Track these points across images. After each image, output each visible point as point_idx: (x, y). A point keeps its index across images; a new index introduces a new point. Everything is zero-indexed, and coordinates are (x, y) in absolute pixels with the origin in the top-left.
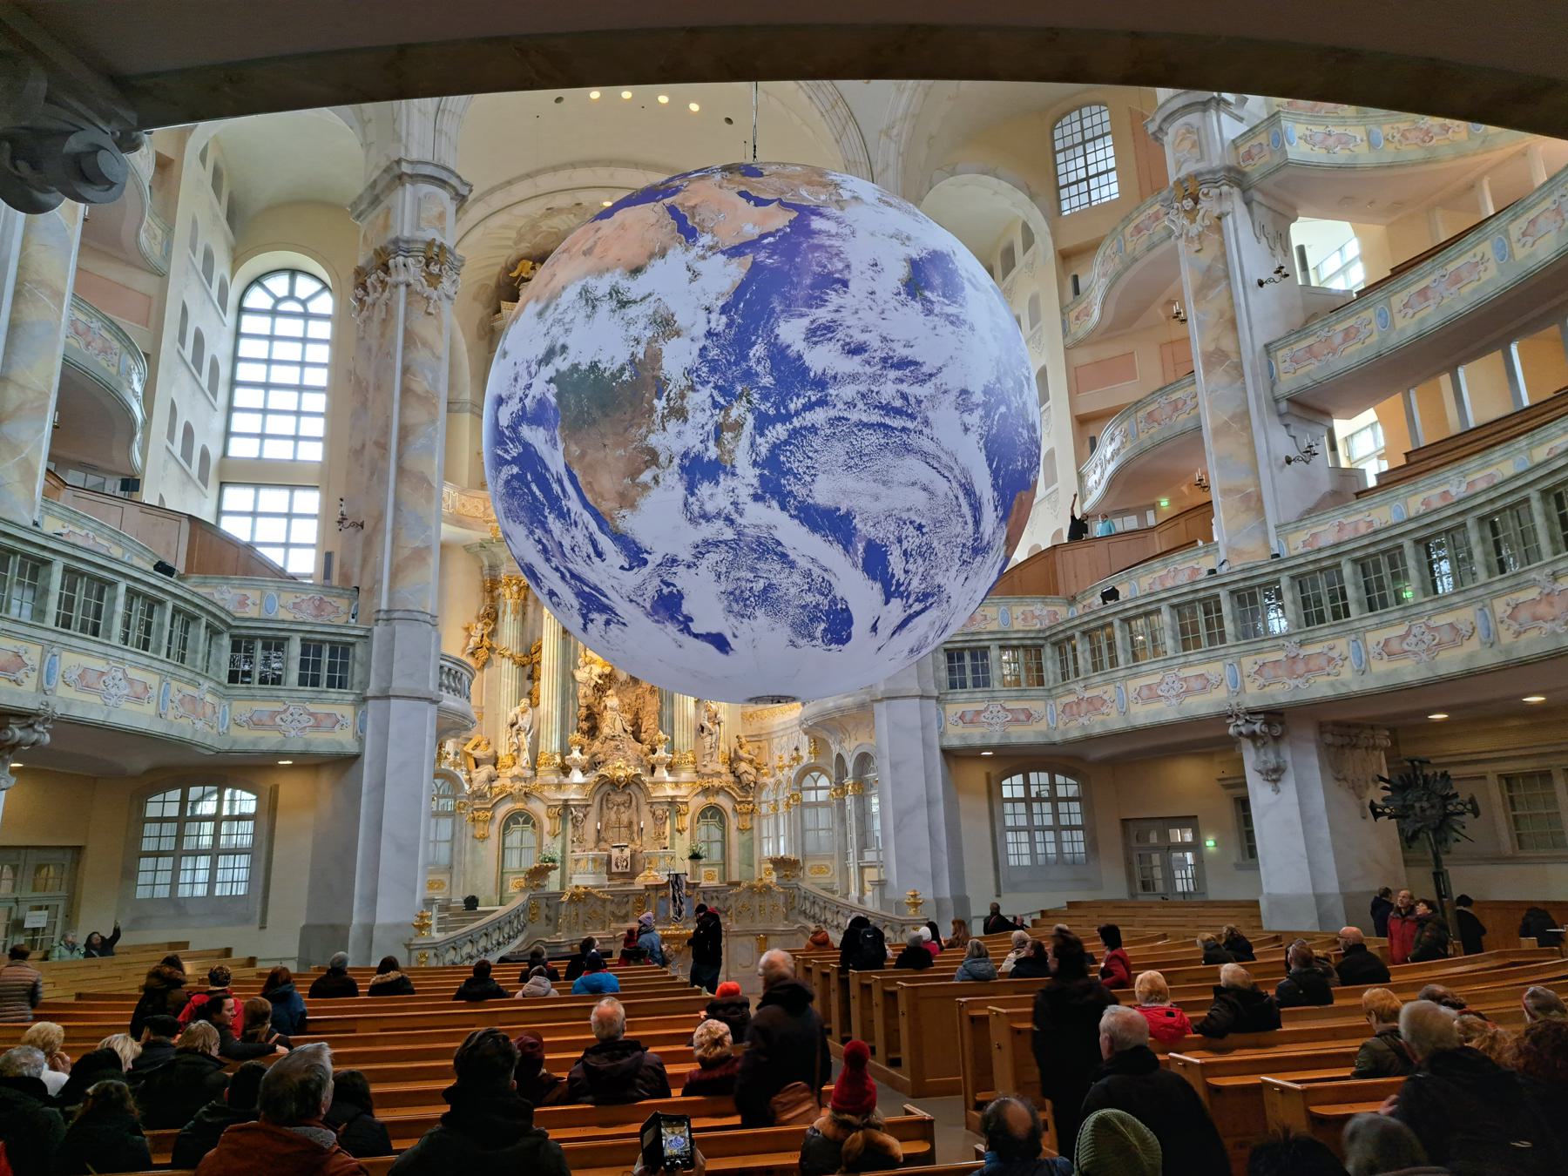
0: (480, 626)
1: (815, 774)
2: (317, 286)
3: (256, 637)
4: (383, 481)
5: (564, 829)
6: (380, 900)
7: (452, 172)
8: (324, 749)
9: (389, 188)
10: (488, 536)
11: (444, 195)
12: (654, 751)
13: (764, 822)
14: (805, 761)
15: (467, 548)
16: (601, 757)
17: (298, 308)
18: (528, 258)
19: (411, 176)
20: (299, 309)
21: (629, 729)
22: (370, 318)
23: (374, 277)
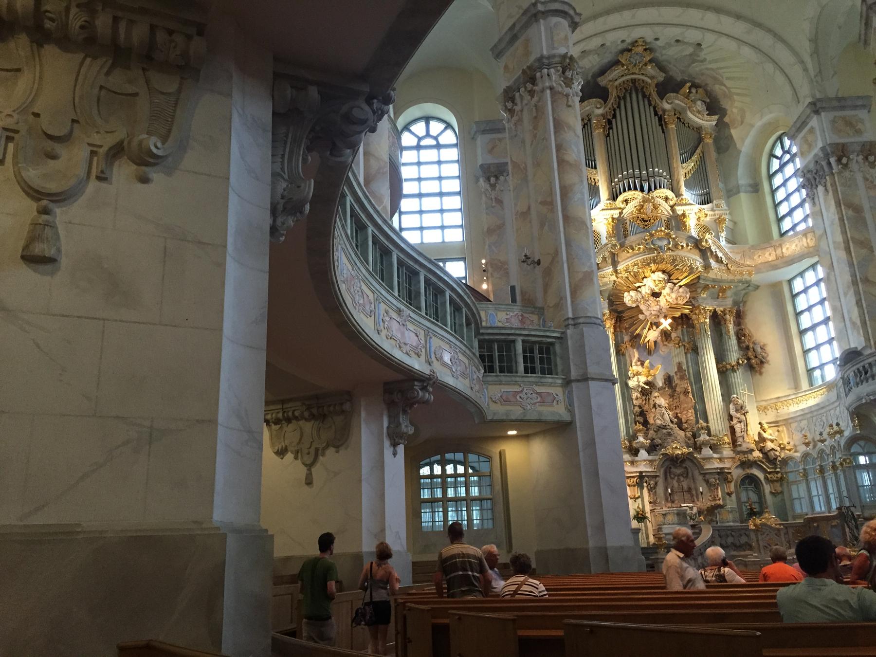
2: (442, 126)
3: (493, 341)
4: (554, 227)
5: (642, 493)
6: (607, 528)
7: (570, 5)
8: (550, 418)
9: (526, 26)
11: (565, 23)
13: (794, 488)
16: (660, 441)
17: (434, 142)
19: (543, 13)
20: (434, 142)
22: (520, 120)
23: (522, 90)
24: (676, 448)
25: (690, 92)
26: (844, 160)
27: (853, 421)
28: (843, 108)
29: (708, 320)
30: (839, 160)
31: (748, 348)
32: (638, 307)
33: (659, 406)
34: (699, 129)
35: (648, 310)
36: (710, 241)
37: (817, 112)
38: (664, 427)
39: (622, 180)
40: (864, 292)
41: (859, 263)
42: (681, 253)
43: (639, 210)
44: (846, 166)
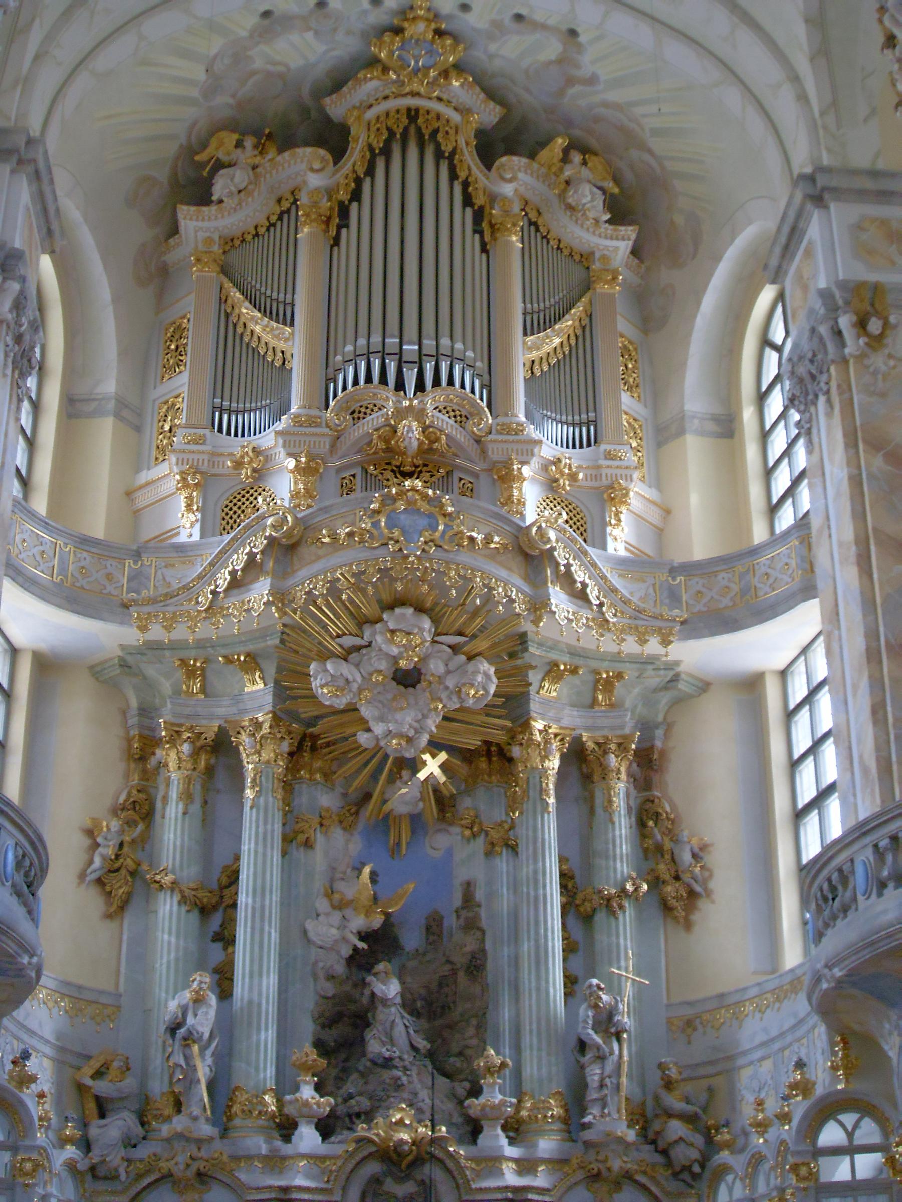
0: (115, 825)
1: (849, 1119)
10: (131, 635)
12: (476, 1091)
14: (819, 1091)
15: (96, 671)
18: (233, 131)
21: (423, 1044)
24: (401, 1122)
25: (565, 159)
26: (875, 325)
27: (835, 1053)
28: (884, 196)
29: (554, 763)
30: (862, 324)
31: (659, 849)
32: (352, 709)
33: (385, 1002)
34: (584, 259)
35: (382, 719)
36: (552, 535)
37: (818, 200)
38: (387, 1063)
39: (353, 360)
40: (894, 680)
41: (886, 599)
42: (464, 557)
43: (387, 441)
44: (877, 342)
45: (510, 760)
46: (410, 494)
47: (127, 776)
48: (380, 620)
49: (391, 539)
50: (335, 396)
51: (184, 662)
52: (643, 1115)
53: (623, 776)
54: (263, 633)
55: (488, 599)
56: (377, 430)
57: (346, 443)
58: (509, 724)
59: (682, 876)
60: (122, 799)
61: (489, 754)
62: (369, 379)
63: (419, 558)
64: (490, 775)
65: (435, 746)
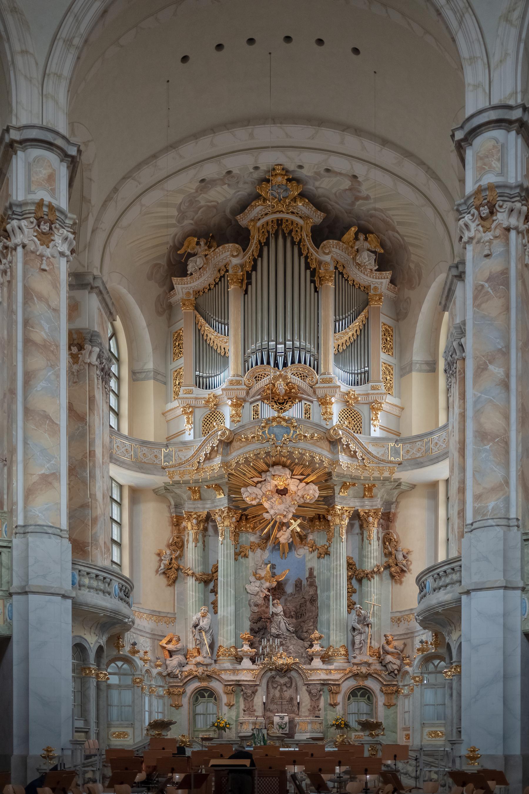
31: (390, 554)
32: (260, 504)
35: (272, 508)
42: (302, 444)
45: (328, 521)
46: (277, 419)
47: (172, 532)
48: (268, 471)
49: (270, 439)
50: (248, 370)
51: (190, 488)
52: (379, 653)
53: (376, 525)
54: (221, 477)
55: (312, 461)
56: (266, 385)
57: (253, 391)
58: (326, 507)
59: (398, 564)
60: (170, 542)
61: (319, 518)
62: (262, 363)
63: (281, 447)
64: (320, 527)
65: (295, 517)
